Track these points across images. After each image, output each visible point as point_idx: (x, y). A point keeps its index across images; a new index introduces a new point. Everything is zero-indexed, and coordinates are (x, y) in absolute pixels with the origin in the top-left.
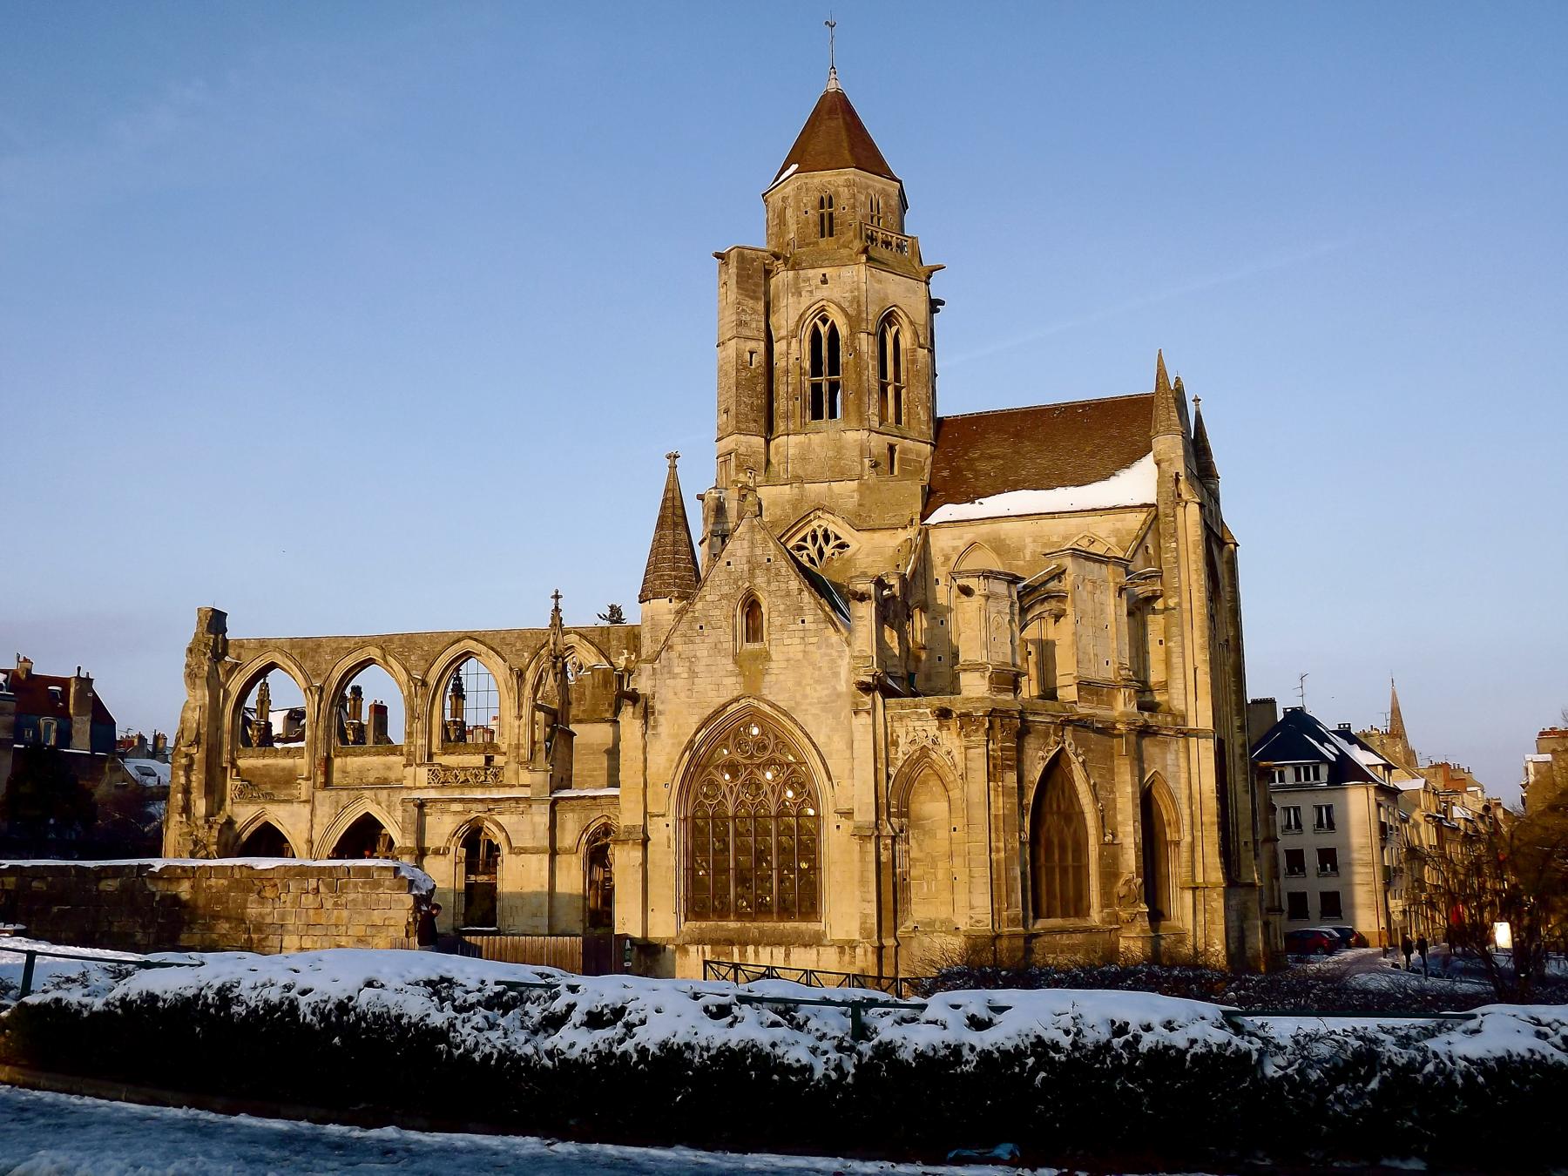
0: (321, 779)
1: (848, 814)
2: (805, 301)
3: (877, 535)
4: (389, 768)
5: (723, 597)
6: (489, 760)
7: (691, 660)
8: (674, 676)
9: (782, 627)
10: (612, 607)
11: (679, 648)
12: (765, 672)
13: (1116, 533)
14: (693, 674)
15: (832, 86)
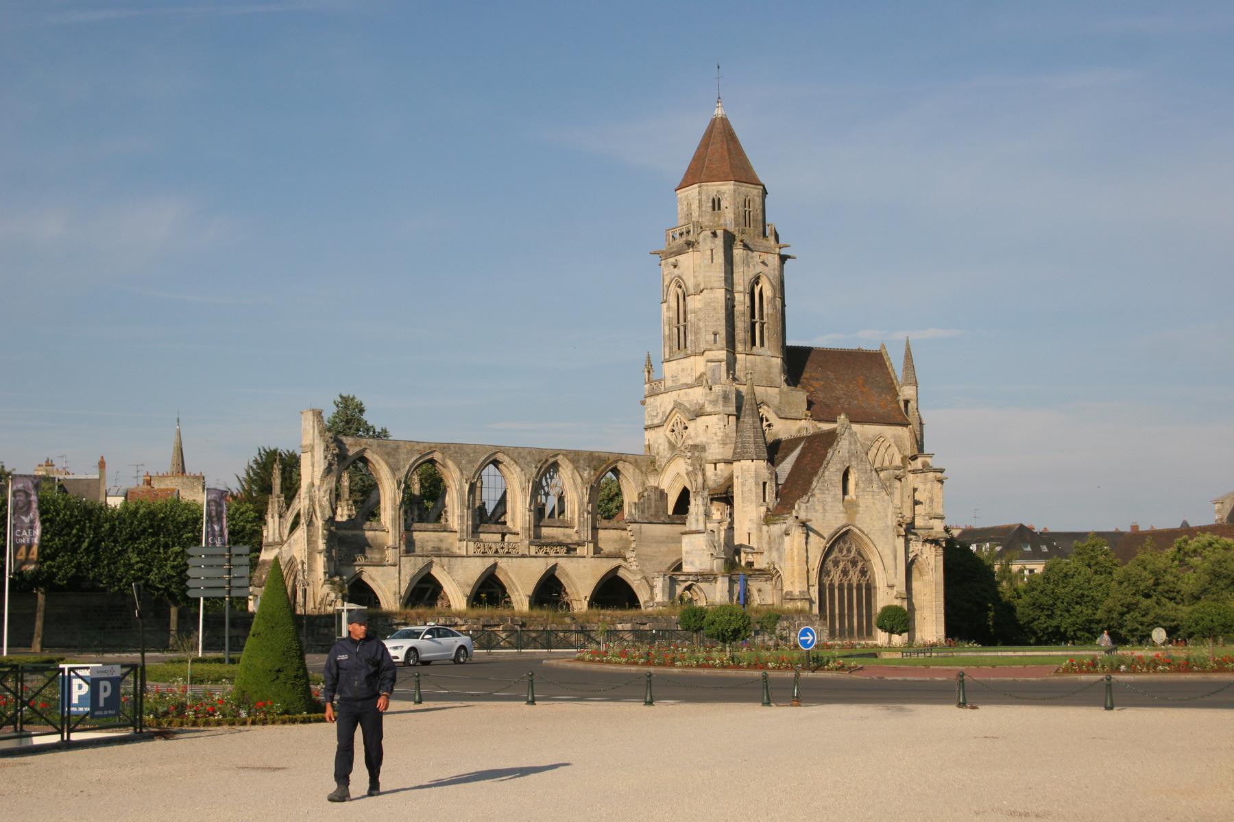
0: (403, 548)
1: (891, 587)
2: (752, 273)
3: (788, 422)
4: (441, 541)
5: (838, 470)
6: (504, 535)
7: (824, 503)
8: (816, 511)
9: (864, 490)
10: (346, 402)
11: (818, 496)
12: (857, 512)
13: (894, 436)
14: (825, 510)
15: (719, 112)
